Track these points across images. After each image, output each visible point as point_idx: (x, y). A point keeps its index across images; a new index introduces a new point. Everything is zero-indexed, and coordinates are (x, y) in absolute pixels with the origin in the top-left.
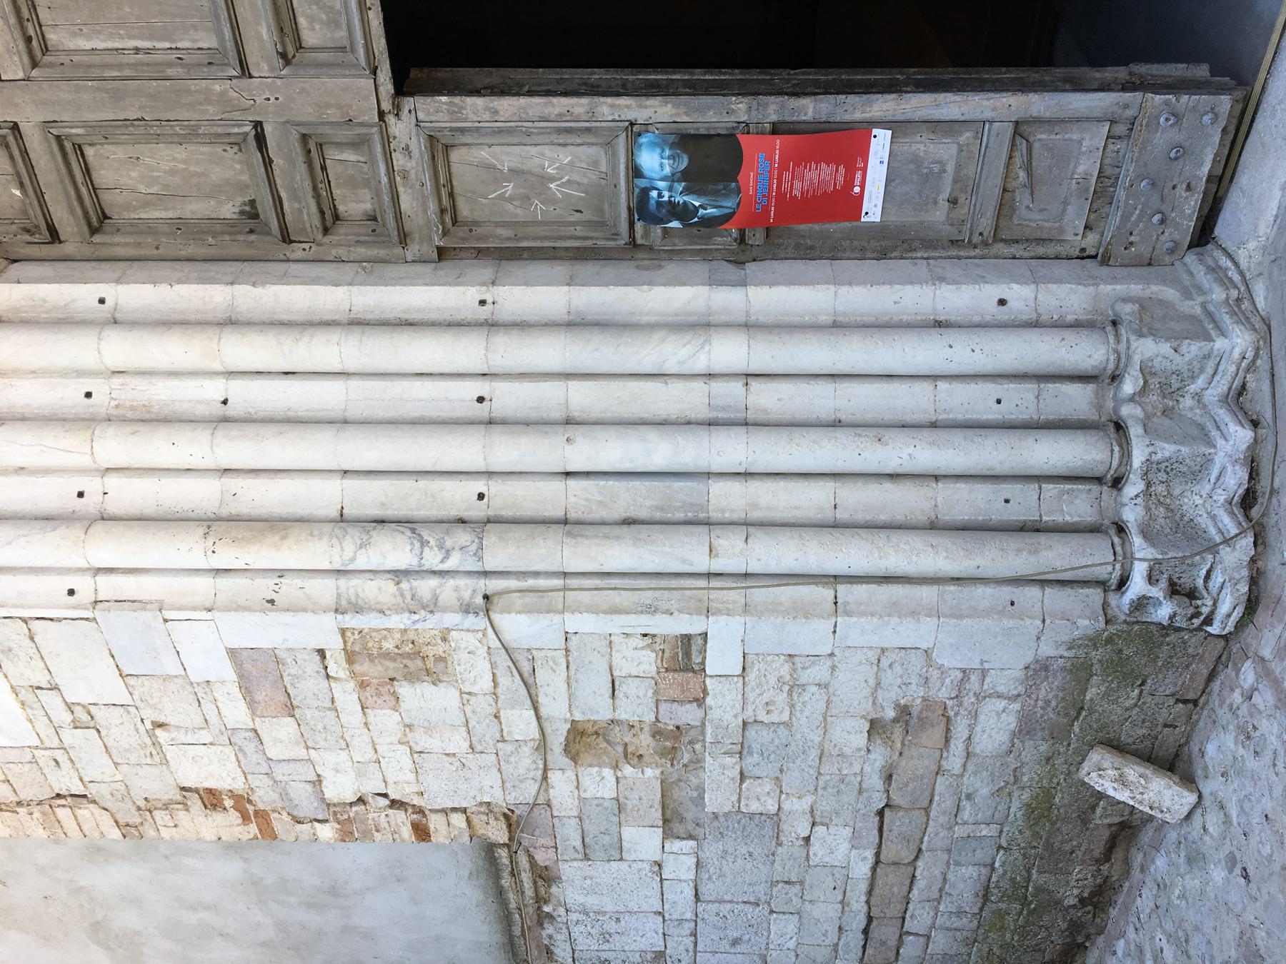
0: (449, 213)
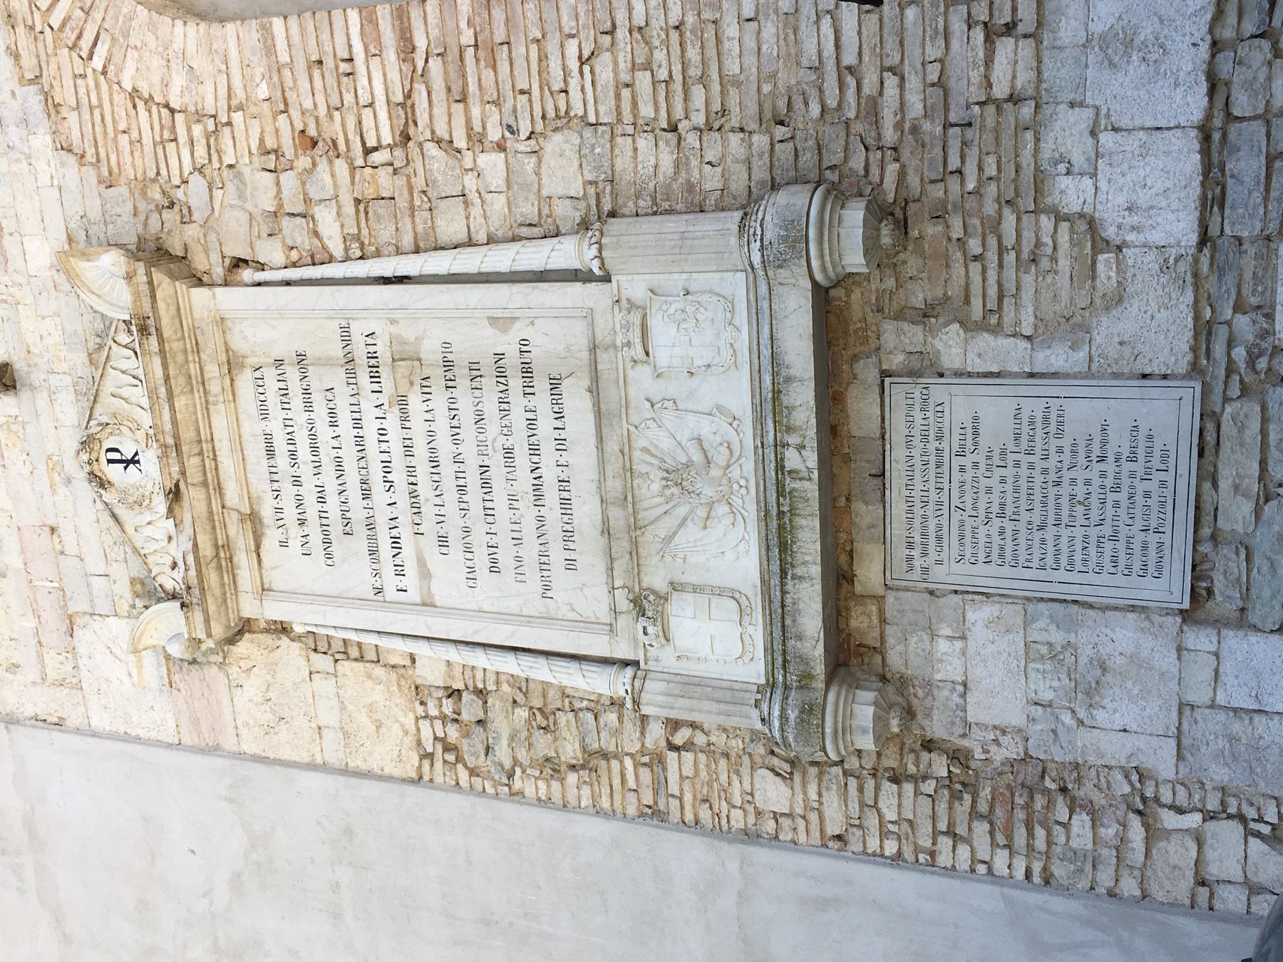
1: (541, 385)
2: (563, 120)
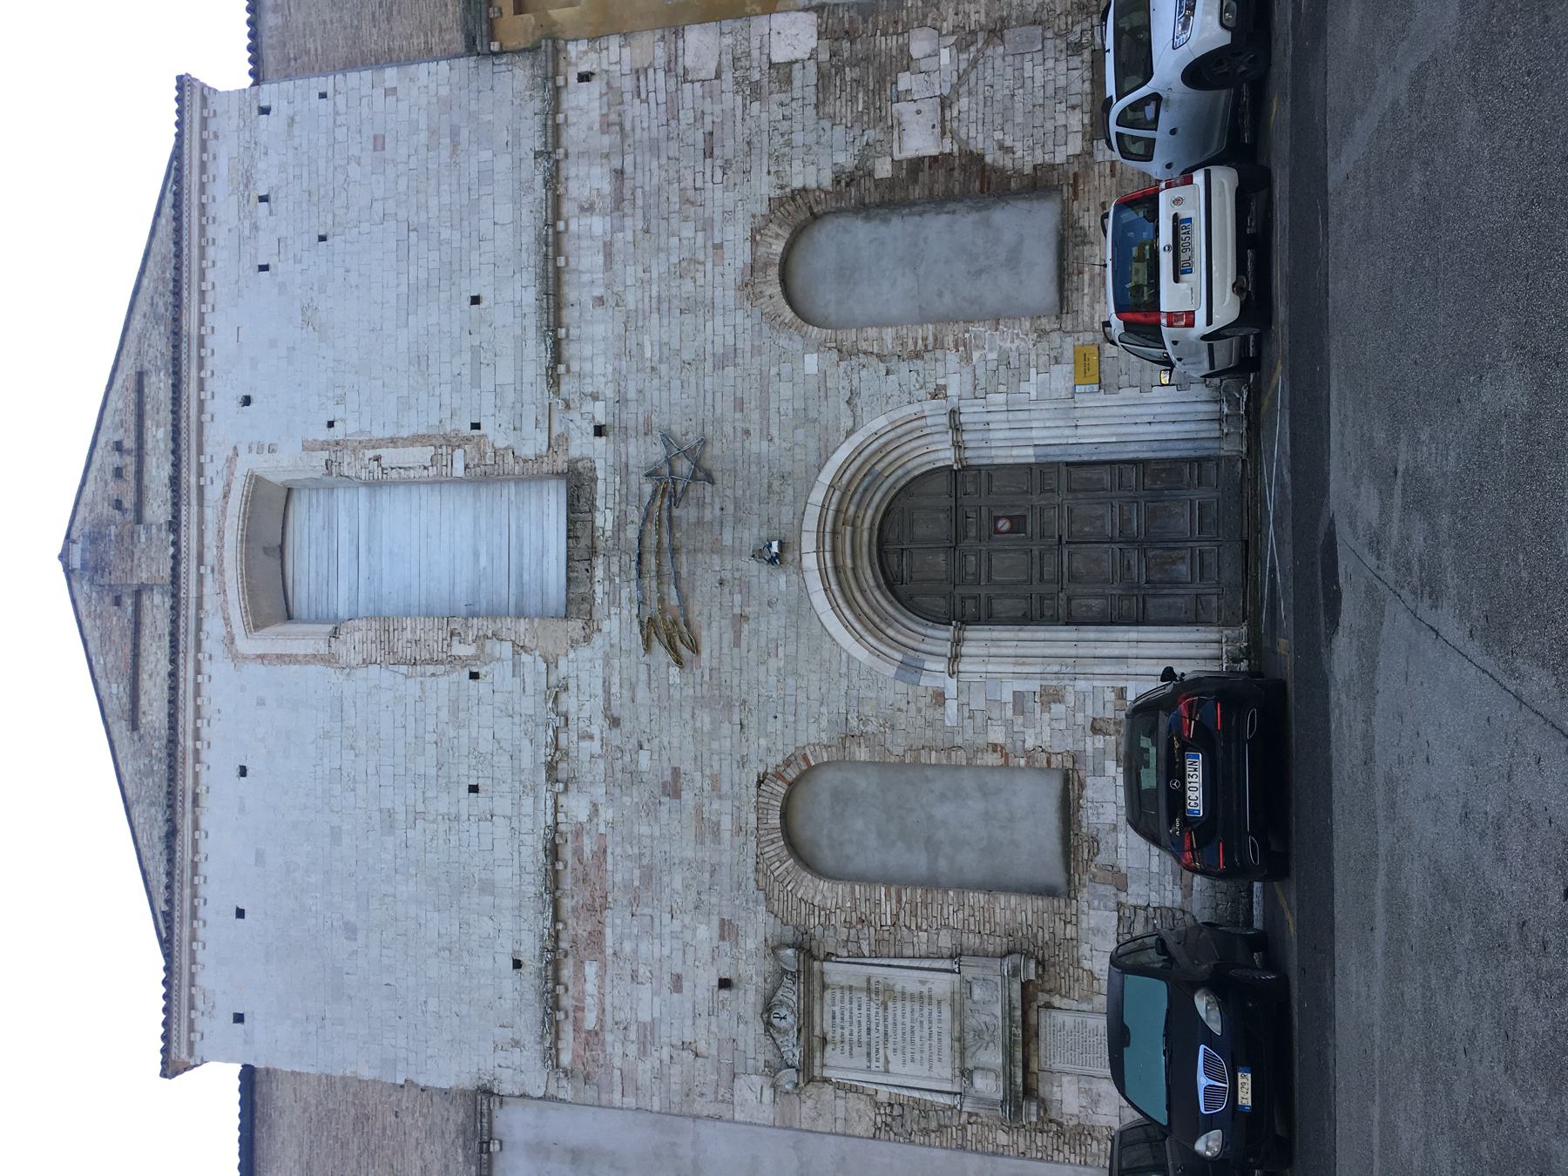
0: (1069, 614)
1: (935, 1002)
2: (947, 926)
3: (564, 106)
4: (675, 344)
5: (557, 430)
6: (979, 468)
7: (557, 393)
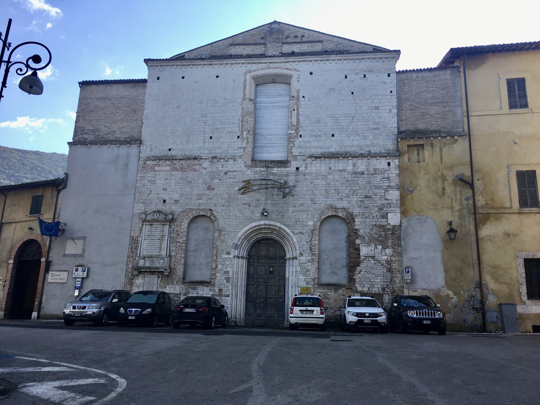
3: (382, 159)
4: (318, 188)
5: (298, 157)
6: (285, 263)
7: (308, 158)
